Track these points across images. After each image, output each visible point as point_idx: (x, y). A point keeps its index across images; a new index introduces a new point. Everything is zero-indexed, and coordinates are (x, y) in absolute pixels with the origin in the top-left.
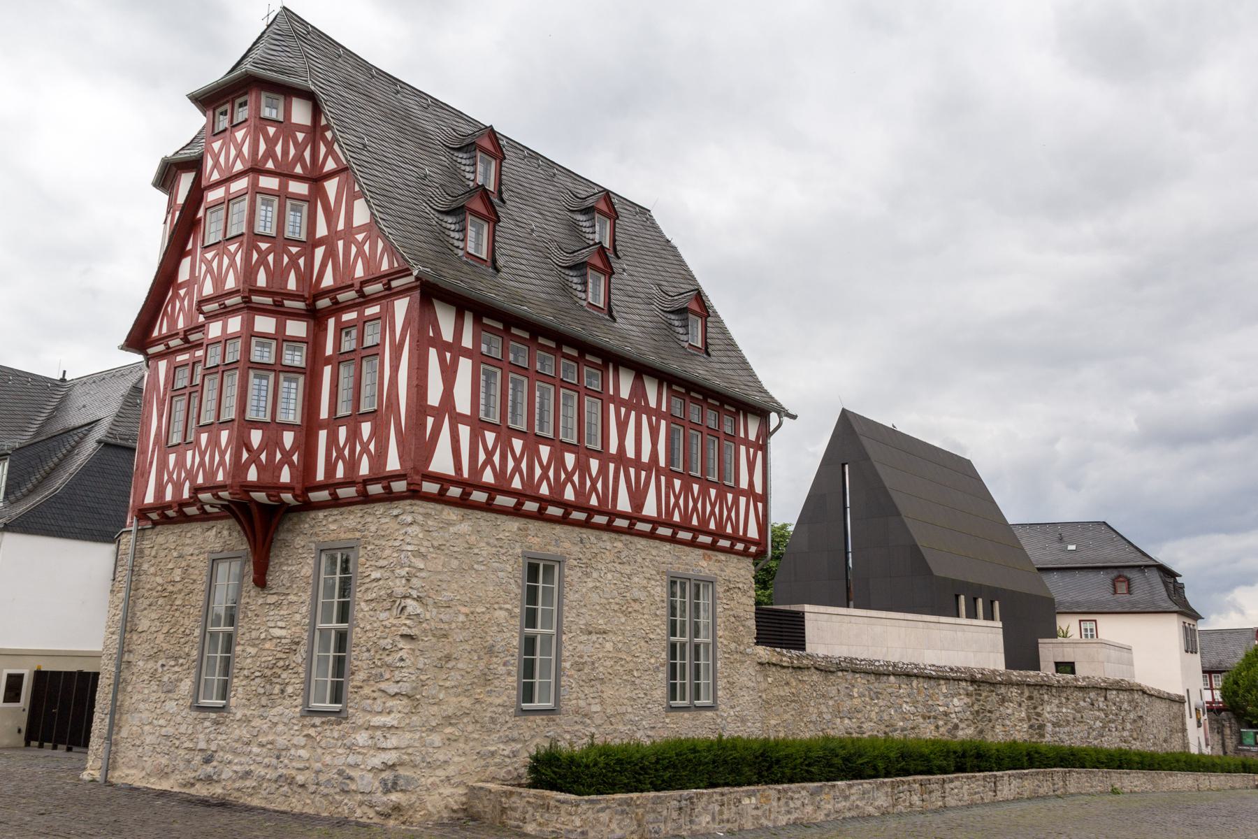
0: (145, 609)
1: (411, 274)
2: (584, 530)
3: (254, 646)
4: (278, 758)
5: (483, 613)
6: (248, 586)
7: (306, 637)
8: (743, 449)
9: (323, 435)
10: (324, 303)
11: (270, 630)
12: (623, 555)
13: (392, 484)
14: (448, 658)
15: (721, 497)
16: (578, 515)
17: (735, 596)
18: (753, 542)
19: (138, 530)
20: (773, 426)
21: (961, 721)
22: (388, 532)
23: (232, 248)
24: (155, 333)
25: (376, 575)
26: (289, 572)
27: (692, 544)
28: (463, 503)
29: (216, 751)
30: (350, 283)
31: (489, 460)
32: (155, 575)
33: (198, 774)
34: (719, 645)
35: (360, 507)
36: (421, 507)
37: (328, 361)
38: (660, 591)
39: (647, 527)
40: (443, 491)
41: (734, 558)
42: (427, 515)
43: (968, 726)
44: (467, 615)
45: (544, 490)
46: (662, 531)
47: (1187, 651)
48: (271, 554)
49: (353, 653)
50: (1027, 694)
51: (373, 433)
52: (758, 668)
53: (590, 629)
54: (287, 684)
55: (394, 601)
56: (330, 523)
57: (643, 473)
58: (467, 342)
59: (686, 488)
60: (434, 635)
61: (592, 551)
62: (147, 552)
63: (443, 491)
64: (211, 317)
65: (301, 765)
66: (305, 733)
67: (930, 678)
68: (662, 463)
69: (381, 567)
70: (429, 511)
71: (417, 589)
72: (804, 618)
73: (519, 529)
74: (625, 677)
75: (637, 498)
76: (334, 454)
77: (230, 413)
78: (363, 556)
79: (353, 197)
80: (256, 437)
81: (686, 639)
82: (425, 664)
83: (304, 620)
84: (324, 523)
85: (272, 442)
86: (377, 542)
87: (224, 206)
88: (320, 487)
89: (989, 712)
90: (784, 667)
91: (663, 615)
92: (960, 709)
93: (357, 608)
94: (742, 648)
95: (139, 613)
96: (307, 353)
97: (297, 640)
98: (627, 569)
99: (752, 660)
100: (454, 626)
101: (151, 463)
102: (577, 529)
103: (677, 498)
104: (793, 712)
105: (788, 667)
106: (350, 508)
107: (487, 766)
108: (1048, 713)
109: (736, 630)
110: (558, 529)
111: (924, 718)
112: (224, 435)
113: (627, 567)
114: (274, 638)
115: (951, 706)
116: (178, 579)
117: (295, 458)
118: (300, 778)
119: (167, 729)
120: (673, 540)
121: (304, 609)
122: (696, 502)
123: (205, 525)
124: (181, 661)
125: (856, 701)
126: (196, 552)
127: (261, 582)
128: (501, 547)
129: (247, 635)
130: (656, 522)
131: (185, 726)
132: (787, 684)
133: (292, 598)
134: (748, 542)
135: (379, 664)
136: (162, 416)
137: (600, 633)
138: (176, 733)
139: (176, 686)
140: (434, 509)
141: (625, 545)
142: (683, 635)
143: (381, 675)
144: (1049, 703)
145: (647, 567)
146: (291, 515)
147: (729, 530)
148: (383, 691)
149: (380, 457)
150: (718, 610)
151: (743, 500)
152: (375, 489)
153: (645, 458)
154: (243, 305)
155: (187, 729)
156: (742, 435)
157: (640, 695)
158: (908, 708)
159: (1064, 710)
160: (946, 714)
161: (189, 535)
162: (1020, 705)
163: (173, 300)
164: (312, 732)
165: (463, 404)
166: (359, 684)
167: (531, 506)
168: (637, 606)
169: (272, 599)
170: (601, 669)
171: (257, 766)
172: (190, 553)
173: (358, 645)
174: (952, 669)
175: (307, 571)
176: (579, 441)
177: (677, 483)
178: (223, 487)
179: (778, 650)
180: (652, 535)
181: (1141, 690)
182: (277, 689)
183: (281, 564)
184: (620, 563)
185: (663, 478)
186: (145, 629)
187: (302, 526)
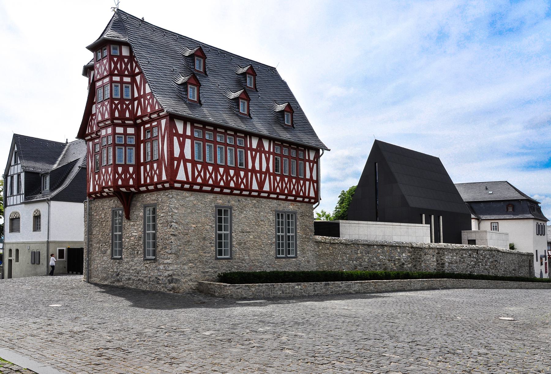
0: (94, 227)
1: (164, 111)
2: (240, 197)
3: (128, 239)
5: (201, 227)
6: (124, 219)
8: (307, 164)
12: (256, 205)
13: (164, 184)
14: (189, 241)
15: (298, 182)
16: (235, 192)
17: (305, 218)
18: (312, 198)
19: (89, 201)
20: (321, 154)
21: (406, 262)
23: (106, 103)
25: (161, 216)
27: (286, 200)
28: (191, 190)
30: (146, 114)
31: (199, 175)
32: (96, 216)
34: (298, 236)
36: (174, 192)
38: (272, 217)
39: (266, 195)
40: (182, 186)
41: (305, 204)
42: (177, 195)
43: (409, 264)
44: (194, 227)
45: (222, 183)
46: (272, 196)
47: (538, 235)
48: (130, 209)
49: (157, 240)
50: (437, 251)
51: (157, 168)
52: (315, 243)
53: (244, 231)
54: (139, 251)
55: (168, 224)
57: (263, 175)
58: (188, 133)
59: (282, 180)
60: (183, 234)
61: (243, 204)
62: (93, 208)
63: (182, 186)
64: (103, 128)
67: (392, 246)
68: (271, 171)
69: (164, 212)
70: (178, 193)
71: (176, 219)
72: (339, 225)
73: (213, 198)
74: (258, 247)
75: (261, 184)
76: (146, 175)
77: (111, 162)
79: (145, 82)
80: (120, 170)
81: (284, 234)
82: (180, 243)
85: (125, 171)
87: (102, 88)
89: (419, 258)
90: (327, 243)
91: (273, 226)
92: (406, 257)
93: (157, 226)
94: (308, 236)
95: (92, 229)
96: (135, 139)
98: (258, 210)
99: (313, 241)
100: (190, 231)
102: (237, 197)
103: (278, 183)
104: (331, 259)
105: (328, 243)
106: (153, 193)
107: (205, 276)
108: (447, 259)
109: (305, 230)
110: (229, 197)
111: (389, 260)
112: (110, 169)
113: (258, 209)
114: (134, 236)
115: (401, 256)
117: (134, 176)
120: (277, 199)
122: (286, 185)
123: (110, 199)
125: (359, 255)
127: (128, 218)
128: (206, 204)
129: (126, 235)
130: (269, 193)
132: (328, 249)
133: (138, 223)
134: (310, 198)
137: (247, 232)
139: (106, 252)
140: (180, 193)
141: (257, 201)
142: (282, 232)
144: (447, 255)
145: (267, 209)
146: (135, 195)
147: (301, 194)
149: (160, 176)
150: (298, 223)
151: (307, 183)
152: (160, 186)
153: (264, 169)
154: (111, 124)
156: (307, 158)
157: (264, 253)
158: (382, 257)
159: (455, 258)
160: (399, 259)
161: (105, 202)
162: (433, 256)
165: (188, 156)
167: (217, 190)
168: (262, 223)
169: (132, 223)
170: (248, 245)
174: (403, 243)
175: (141, 214)
176: (235, 166)
177: (278, 178)
178: (111, 187)
179: (325, 237)
180: (268, 197)
181: (496, 250)
184: (255, 208)
185: (272, 177)
186: (95, 234)
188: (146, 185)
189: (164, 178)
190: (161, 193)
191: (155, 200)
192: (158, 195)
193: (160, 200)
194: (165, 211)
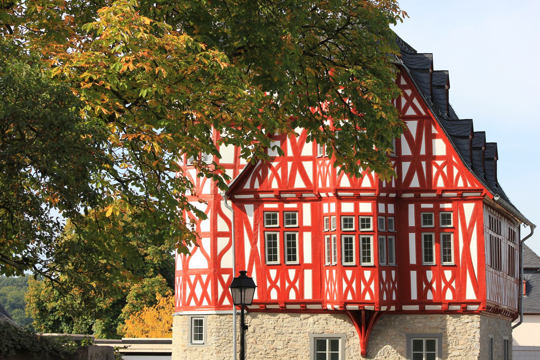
9: (413, 274)
10: (406, 195)
24: (247, 186)
25: (454, 353)
37: (412, 230)
76: (424, 286)
84: (411, 322)
88: (414, 303)
106: (431, 315)
116: (280, 347)
117: (396, 285)
126: (295, 332)
136: (256, 243)
172: (290, 331)
183: (377, 344)
187: (392, 323)
191: (437, 328)
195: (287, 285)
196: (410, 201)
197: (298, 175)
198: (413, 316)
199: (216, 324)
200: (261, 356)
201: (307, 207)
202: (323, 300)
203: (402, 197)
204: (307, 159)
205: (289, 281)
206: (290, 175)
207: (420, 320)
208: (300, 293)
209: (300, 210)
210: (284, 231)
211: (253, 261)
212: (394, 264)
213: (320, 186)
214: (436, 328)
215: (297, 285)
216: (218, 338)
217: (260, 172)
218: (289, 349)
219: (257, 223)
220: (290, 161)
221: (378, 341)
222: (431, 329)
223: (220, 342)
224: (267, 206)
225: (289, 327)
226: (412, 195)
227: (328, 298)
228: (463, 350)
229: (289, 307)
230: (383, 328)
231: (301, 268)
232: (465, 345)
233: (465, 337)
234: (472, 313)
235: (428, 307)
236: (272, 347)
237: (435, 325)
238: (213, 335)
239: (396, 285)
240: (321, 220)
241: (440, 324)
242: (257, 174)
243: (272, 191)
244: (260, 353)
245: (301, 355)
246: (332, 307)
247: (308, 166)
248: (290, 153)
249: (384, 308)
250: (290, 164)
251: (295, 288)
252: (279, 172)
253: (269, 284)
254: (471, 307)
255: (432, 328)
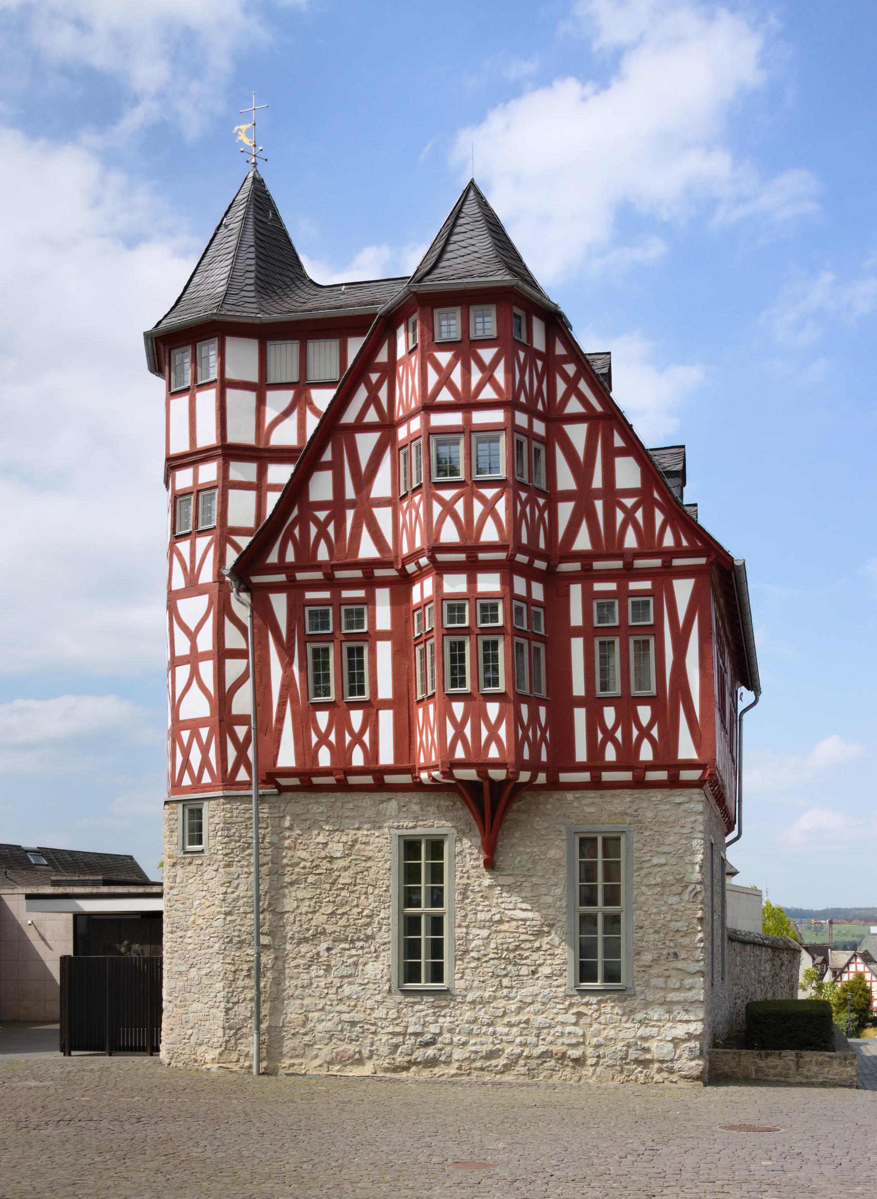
4: (538, 1036)
7: (564, 920)
9: (580, 715)
10: (566, 567)
11: (506, 912)
22: (672, 819)
24: (273, 558)
25: (655, 861)
26: (528, 853)
29: (440, 1034)
33: (413, 1057)
35: (629, 791)
37: (577, 632)
55: (686, 887)
56: (585, 805)
65: (574, 1041)
66: (575, 1010)
76: (600, 736)
78: (638, 841)
83: (559, 903)
84: (576, 804)
86: (655, 828)
97: (552, 922)
101: (281, 719)
106: (613, 791)
114: (513, 919)
116: (338, 855)
117: (548, 735)
118: (574, 1053)
119: (351, 1014)
121: (559, 891)
124: (359, 944)
131: (385, 1011)
135: (672, 944)
136: (291, 663)
138: (368, 1018)
143: (675, 954)
148: (678, 969)
155: (387, 1014)
161: (351, 806)
163: (303, 521)
164: (582, 1009)
166: (648, 964)
171: (505, 1044)
173: (641, 928)
182: (524, 971)
183: (512, 846)
187: (541, 806)
188: (595, 763)
189: (687, 750)
190: (651, 795)
192: (637, 800)
193: (650, 814)
194: (671, 849)
195: (348, 738)
196: (573, 577)
197: (365, 535)
198: (578, 794)
199: (222, 814)
200: (303, 871)
201: (383, 595)
202: (414, 767)
203: (558, 570)
204: (381, 503)
205: (351, 732)
206: (351, 535)
207: (591, 801)
208: (372, 753)
209: (370, 601)
210: (341, 641)
211: (286, 698)
212: (543, 694)
213: (405, 550)
214: (622, 815)
215: (366, 738)
216: (226, 840)
217: (297, 531)
218: (353, 857)
219: (291, 628)
220: (351, 508)
221: (514, 841)
222: (613, 817)
223: (231, 847)
224: (310, 595)
225: (353, 818)
226: (576, 566)
227: (422, 760)
228: (671, 855)
229: (353, 780)
230: (524, 817)
231: (371, 708)
232: (677, 845)
233: (677, 830)
234: (689, 785)
235: (607, 776)
236: (323, 854)
237: (620, 809)
238: (219, 834)
239: (548, 735)
240: (409, 618)
241: (629, 807)
242: (289, 535)
243: (318, 566)
244: (301, 865)
245: (375, 868)
246: (430, 776)
247: (383, 516)
248: (350, 493)
249: (524, 776)
250: (350, 514)
251: (363, 745)
252: (331, 529)
253: (315, 739)
254: (686, 775)
255: (615, 814)
